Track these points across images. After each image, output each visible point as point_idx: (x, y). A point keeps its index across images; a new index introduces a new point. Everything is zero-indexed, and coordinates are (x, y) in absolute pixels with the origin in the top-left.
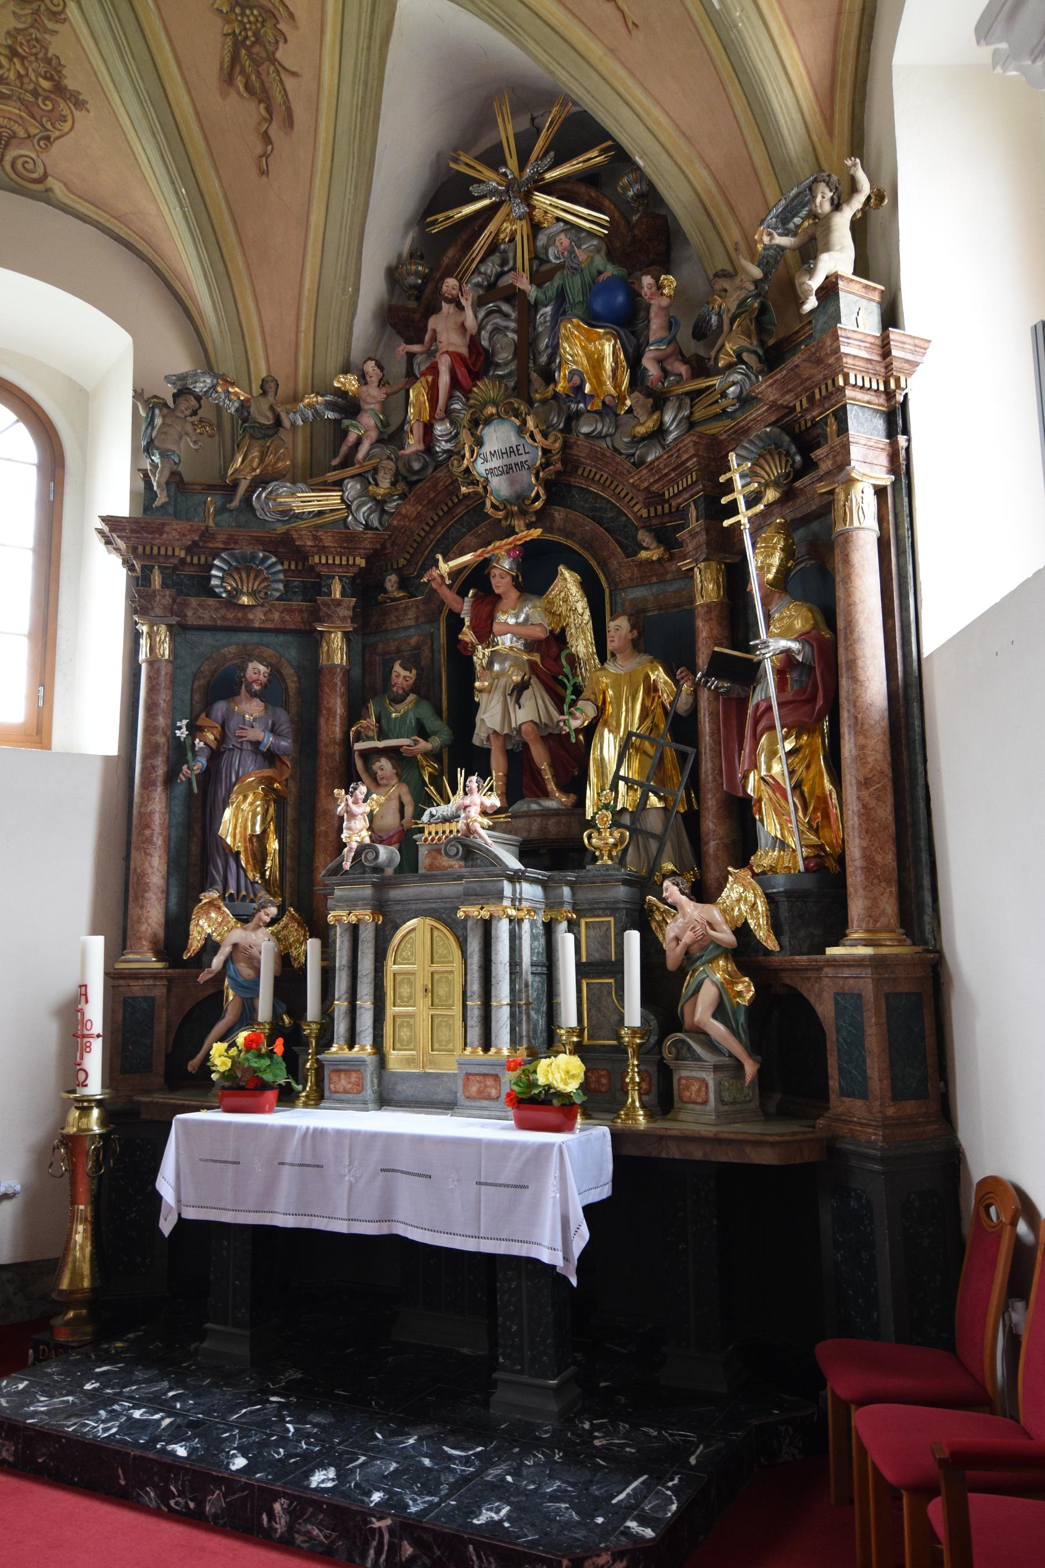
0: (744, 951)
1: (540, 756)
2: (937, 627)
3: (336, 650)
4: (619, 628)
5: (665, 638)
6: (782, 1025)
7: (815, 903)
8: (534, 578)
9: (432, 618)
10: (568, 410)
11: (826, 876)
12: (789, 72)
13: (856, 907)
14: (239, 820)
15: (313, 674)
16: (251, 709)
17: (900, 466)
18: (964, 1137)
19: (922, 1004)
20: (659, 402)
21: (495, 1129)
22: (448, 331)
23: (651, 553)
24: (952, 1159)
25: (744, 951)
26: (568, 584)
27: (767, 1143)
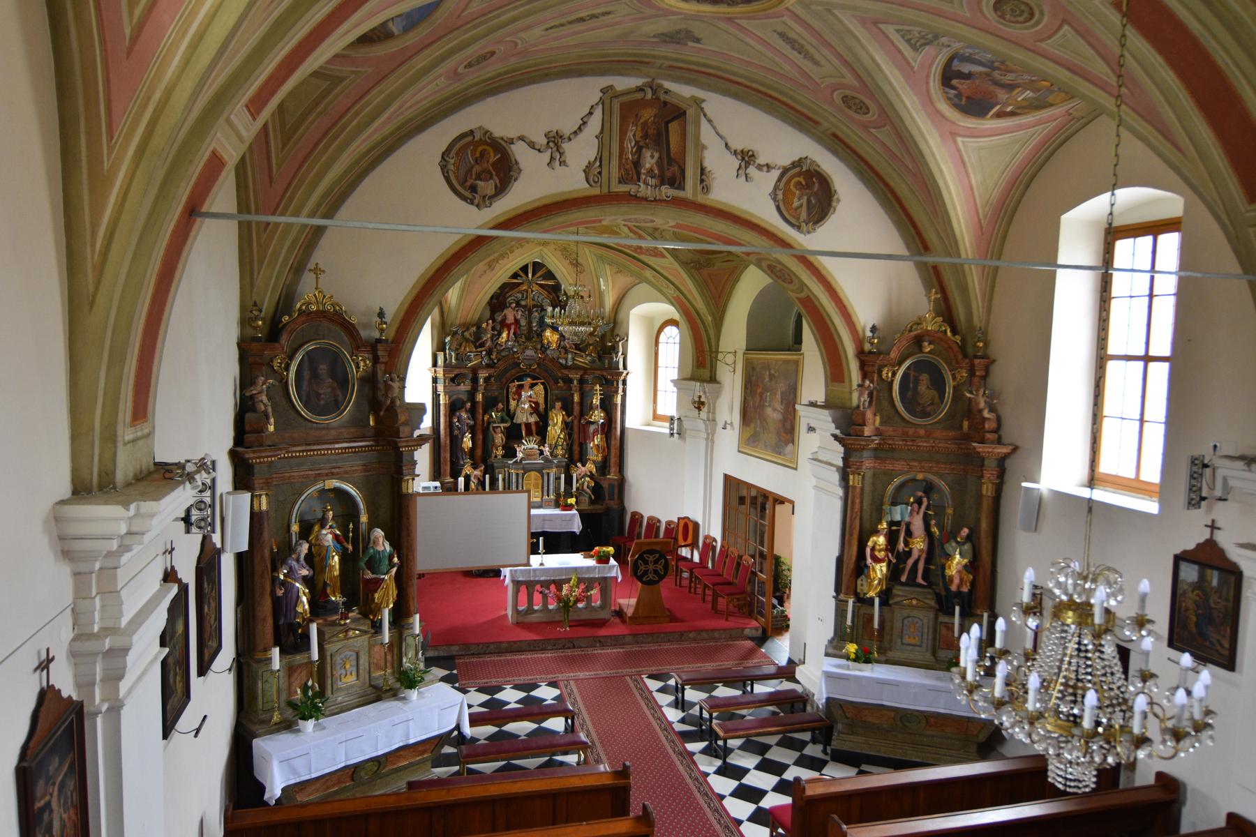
0: (591, 476)
1: (534, 428)
2: (628, 424)
3: (479, 397)
4: (558, 405)
5: (567, 409)
6: (597, 489)
7: (603, 467)
8: (532, 386)
9: (502, 389)
10: (544, 349)
11: (605, 460)
12: (609, 302)
13: (613, 470)
14: (467, 442)
15: (474, 403)
16: (464, 415)
17: (624, 391)
18: (626, 504)
19: (621, 485)
20: (566, 352)
21: (558, 511)
22: (510, 315)
23: (561, 384)
24: (623, 510)
25: (591, 476)
26: (540, 388)
27: (599, 508)
